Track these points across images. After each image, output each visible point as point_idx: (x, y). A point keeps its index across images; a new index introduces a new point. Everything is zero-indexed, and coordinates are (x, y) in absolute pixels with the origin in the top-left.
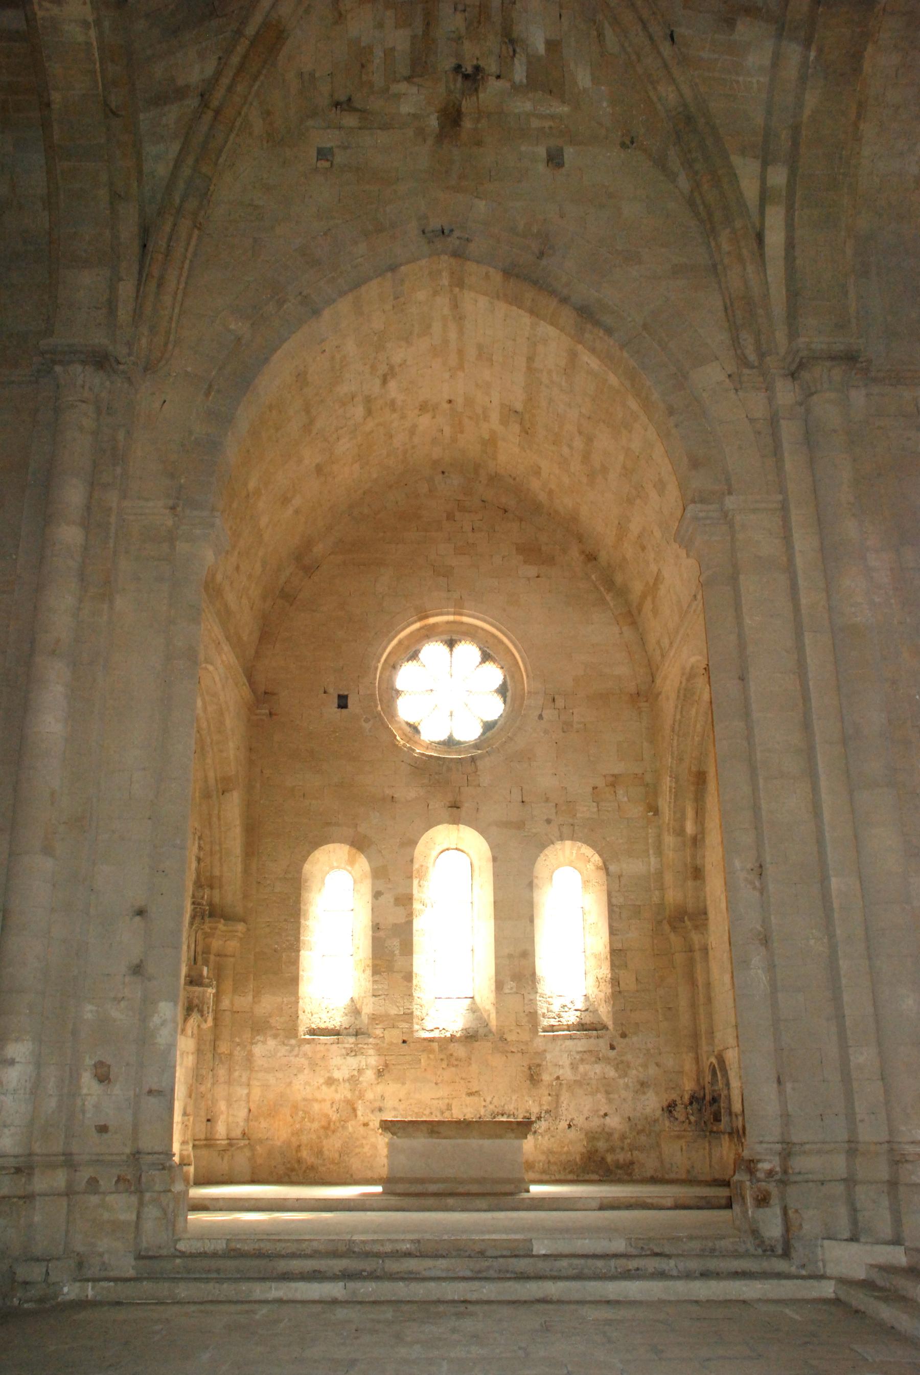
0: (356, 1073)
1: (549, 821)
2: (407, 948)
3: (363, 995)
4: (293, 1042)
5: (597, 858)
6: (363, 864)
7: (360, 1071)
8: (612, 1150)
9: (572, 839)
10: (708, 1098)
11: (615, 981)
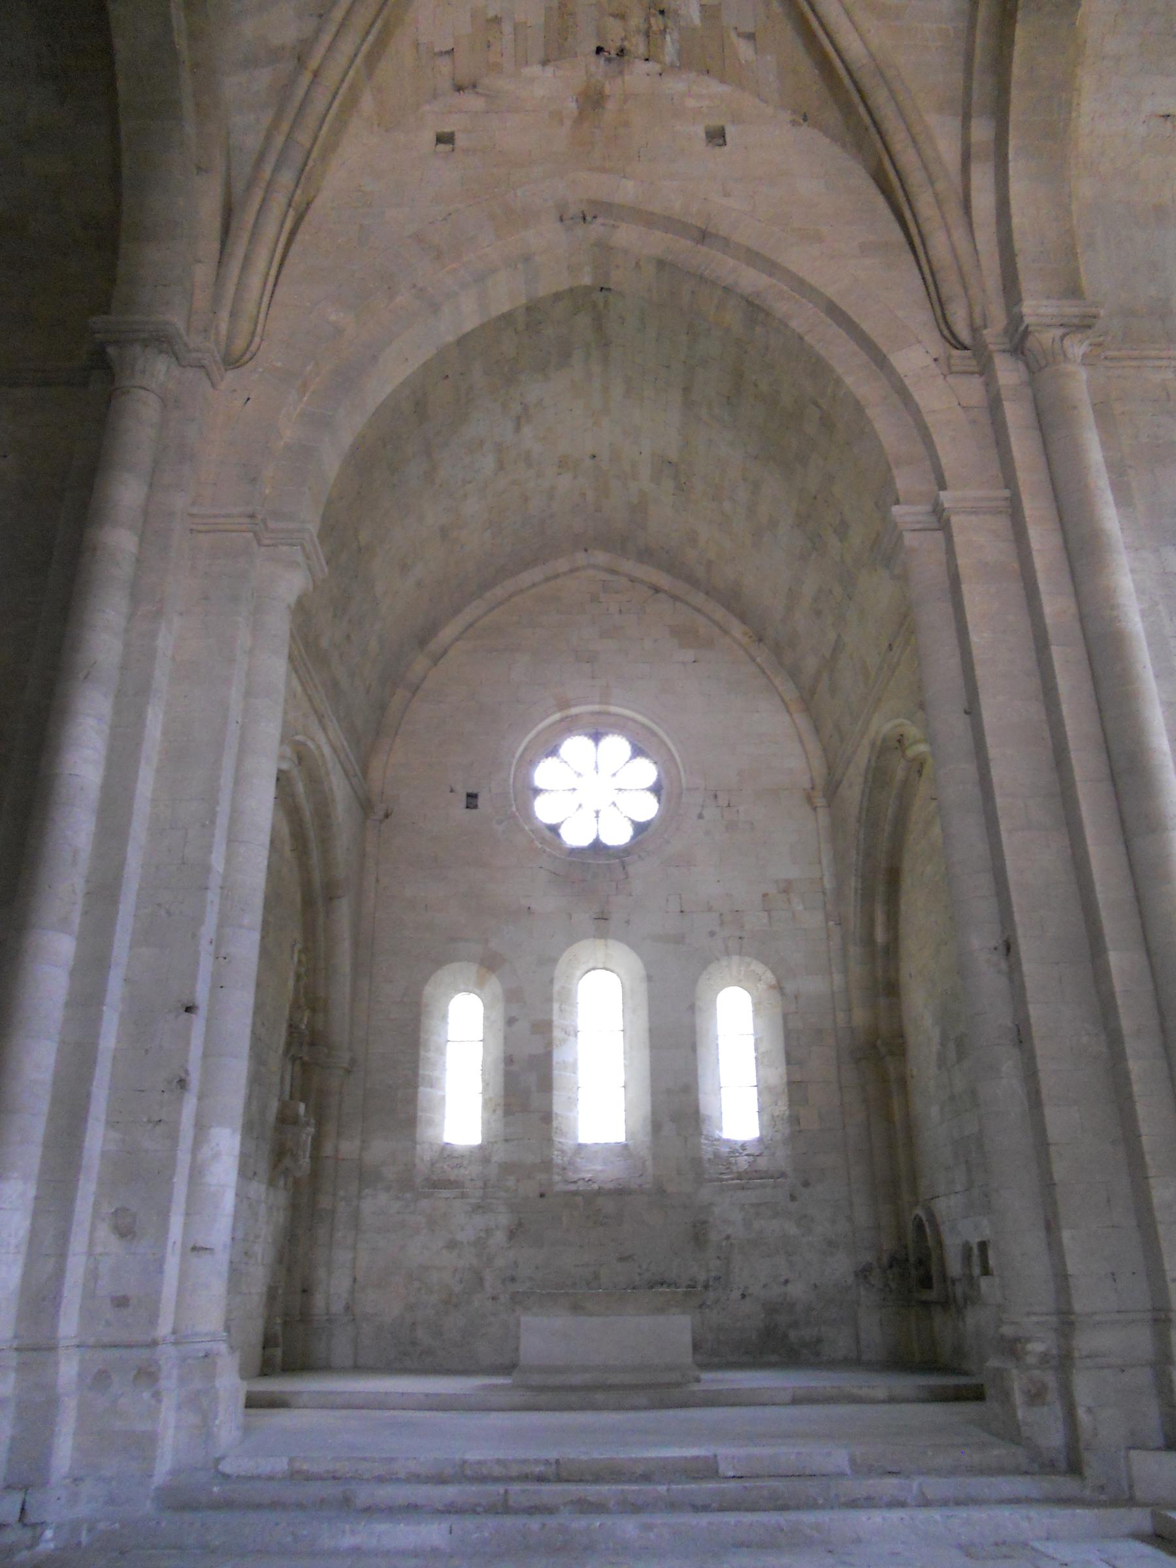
0: (483, 1234)
1: (712, 934)
2: (546, 1084)
3: (492, 1140)
4: (408, 1195)
5: (769, 976)
6: (494, 985)
7: (489, 1232)
9: (740, 953)
10: (912, 1259)
11: (794, 1119)
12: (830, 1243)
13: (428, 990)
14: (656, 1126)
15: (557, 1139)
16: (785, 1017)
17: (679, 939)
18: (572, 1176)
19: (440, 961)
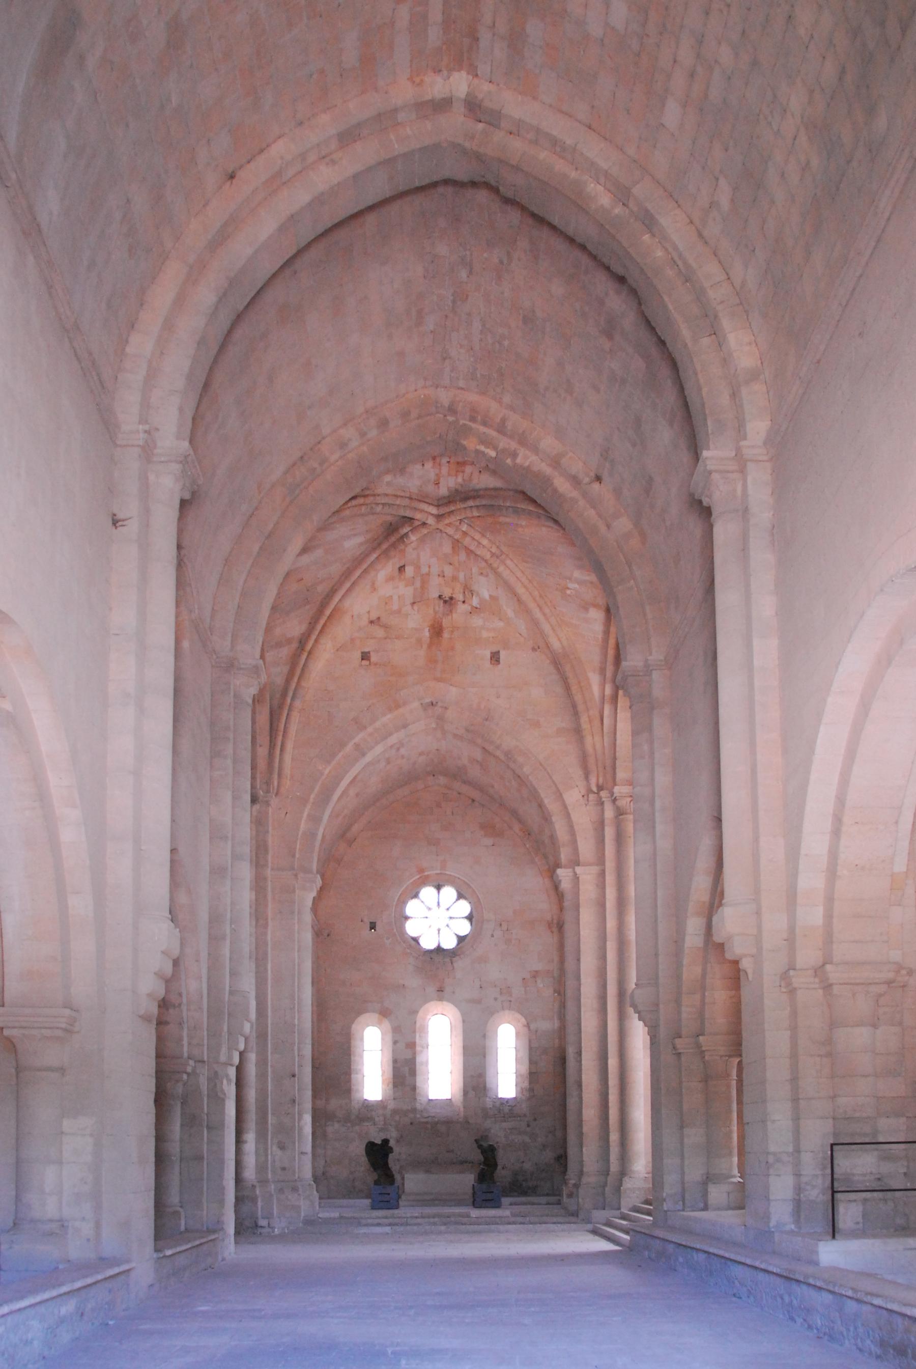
1: (496, 999)
2: (413, 1072)
5: (523, 1020)
6: (387, 1024)
8: (526, 1180)
11: (531, 1090)
13: (354, 1026)
14: (465, 1093)
15: (418, 1098)
16: (530, 1041)
17: (478, 1001)
18: (426, 1115)
19: (359, 1013)
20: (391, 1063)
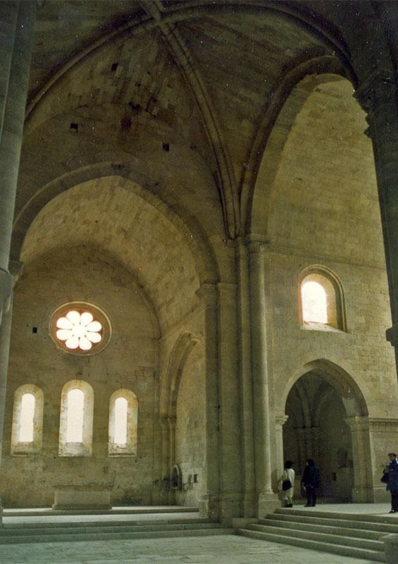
2: (58, 425)
4: (8, 457)
5: (134, 396)
6: (40, 392)
7: (36, 468)
9: (125, 388)
12: (146, 474)
13: (17, 392)
15: (60, 441)
17: (106, 383)
19: (21, 384)
20: (42, 418)
